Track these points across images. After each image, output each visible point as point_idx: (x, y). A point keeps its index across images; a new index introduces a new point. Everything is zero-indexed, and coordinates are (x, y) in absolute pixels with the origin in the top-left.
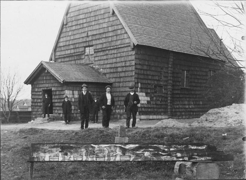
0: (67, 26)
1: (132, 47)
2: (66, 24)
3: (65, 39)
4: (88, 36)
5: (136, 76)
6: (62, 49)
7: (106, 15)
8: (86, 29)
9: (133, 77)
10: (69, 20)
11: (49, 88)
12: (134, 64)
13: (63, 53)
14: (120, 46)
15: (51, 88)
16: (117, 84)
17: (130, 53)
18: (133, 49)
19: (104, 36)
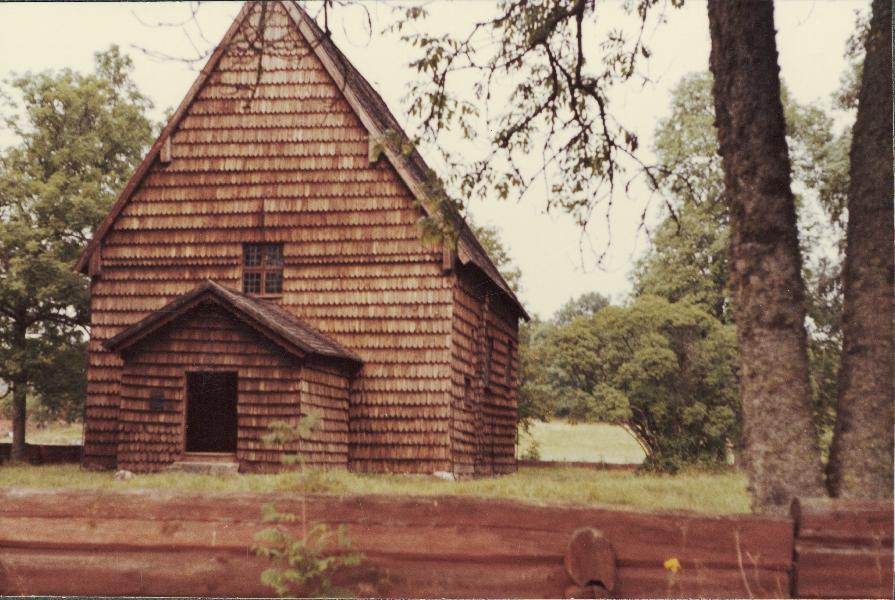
0: (169, 169)
1: (448, 265)
2: (167, 164)
3: (153, 209)
4: (260, 214)
5: (453, 349)
6: (141, 239)
7: (348, 163)
8: (256, 192)
9: (446, 353)
10: (184, 151)
11: (223, 369)
12: (450, 315)
13: (139, 253)
14: (396, 259)
15: (235, 369)
16: (380, 371)
17: (433, 283)
18: (447, 274)
19: (332, 220)
